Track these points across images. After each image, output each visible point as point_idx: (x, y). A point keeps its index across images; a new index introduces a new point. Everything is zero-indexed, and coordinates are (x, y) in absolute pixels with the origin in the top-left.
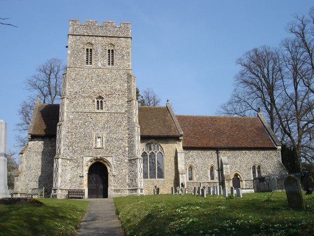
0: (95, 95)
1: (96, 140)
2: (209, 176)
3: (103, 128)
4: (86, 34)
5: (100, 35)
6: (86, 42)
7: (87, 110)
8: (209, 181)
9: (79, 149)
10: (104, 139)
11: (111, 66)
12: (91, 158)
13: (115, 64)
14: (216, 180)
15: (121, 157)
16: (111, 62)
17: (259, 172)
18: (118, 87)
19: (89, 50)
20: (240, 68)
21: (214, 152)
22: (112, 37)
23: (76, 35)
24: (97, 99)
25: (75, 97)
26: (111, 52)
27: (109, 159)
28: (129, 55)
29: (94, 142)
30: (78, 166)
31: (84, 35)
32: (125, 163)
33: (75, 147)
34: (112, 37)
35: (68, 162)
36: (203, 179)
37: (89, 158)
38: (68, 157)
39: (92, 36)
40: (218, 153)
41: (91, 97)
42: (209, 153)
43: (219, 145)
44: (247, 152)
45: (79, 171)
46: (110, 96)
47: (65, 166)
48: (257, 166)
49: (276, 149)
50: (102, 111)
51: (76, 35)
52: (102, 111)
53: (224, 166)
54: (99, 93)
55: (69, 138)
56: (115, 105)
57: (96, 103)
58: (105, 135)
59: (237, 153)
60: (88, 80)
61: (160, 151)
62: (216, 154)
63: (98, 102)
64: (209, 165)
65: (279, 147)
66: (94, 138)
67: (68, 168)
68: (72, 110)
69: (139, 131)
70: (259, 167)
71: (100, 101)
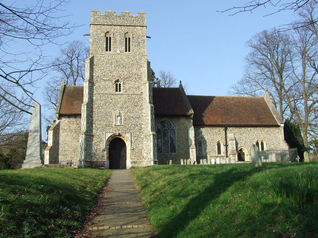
0: (114, 79)
2: (217, 151)
3: (122, 108)
4: (106, 24)
5: (119, 24)
7: (106, 92)
11: (128, 52)
13: (131, 51)
15: (138, 133)
16: (127, 48)
17: (263, 148)
19: (109, 39)
20: (250, 50)
21: (222, 130)
23: (97, 25)
26: (127, 41)
28: (144, 42)
29: (114, 120)
31: (104, 25)
32: (141, 139)
37: (110, 134)
39: (111, 25)
40: (226, 130)
41: (112, 81)
42: (217, 130)
43: (227, 123)
46: (128, 79)
47: (89, 141)
49: (280, 126)
50: (120, 93)
51: (97, 25)
52: (120, 93)
59: (243, 130)
60: (108, 65)
61: (172, 128)
62: (224, 131)
65: (282, 125)
69: (154, 110)
70: (262, 144)
71: (118, 84)
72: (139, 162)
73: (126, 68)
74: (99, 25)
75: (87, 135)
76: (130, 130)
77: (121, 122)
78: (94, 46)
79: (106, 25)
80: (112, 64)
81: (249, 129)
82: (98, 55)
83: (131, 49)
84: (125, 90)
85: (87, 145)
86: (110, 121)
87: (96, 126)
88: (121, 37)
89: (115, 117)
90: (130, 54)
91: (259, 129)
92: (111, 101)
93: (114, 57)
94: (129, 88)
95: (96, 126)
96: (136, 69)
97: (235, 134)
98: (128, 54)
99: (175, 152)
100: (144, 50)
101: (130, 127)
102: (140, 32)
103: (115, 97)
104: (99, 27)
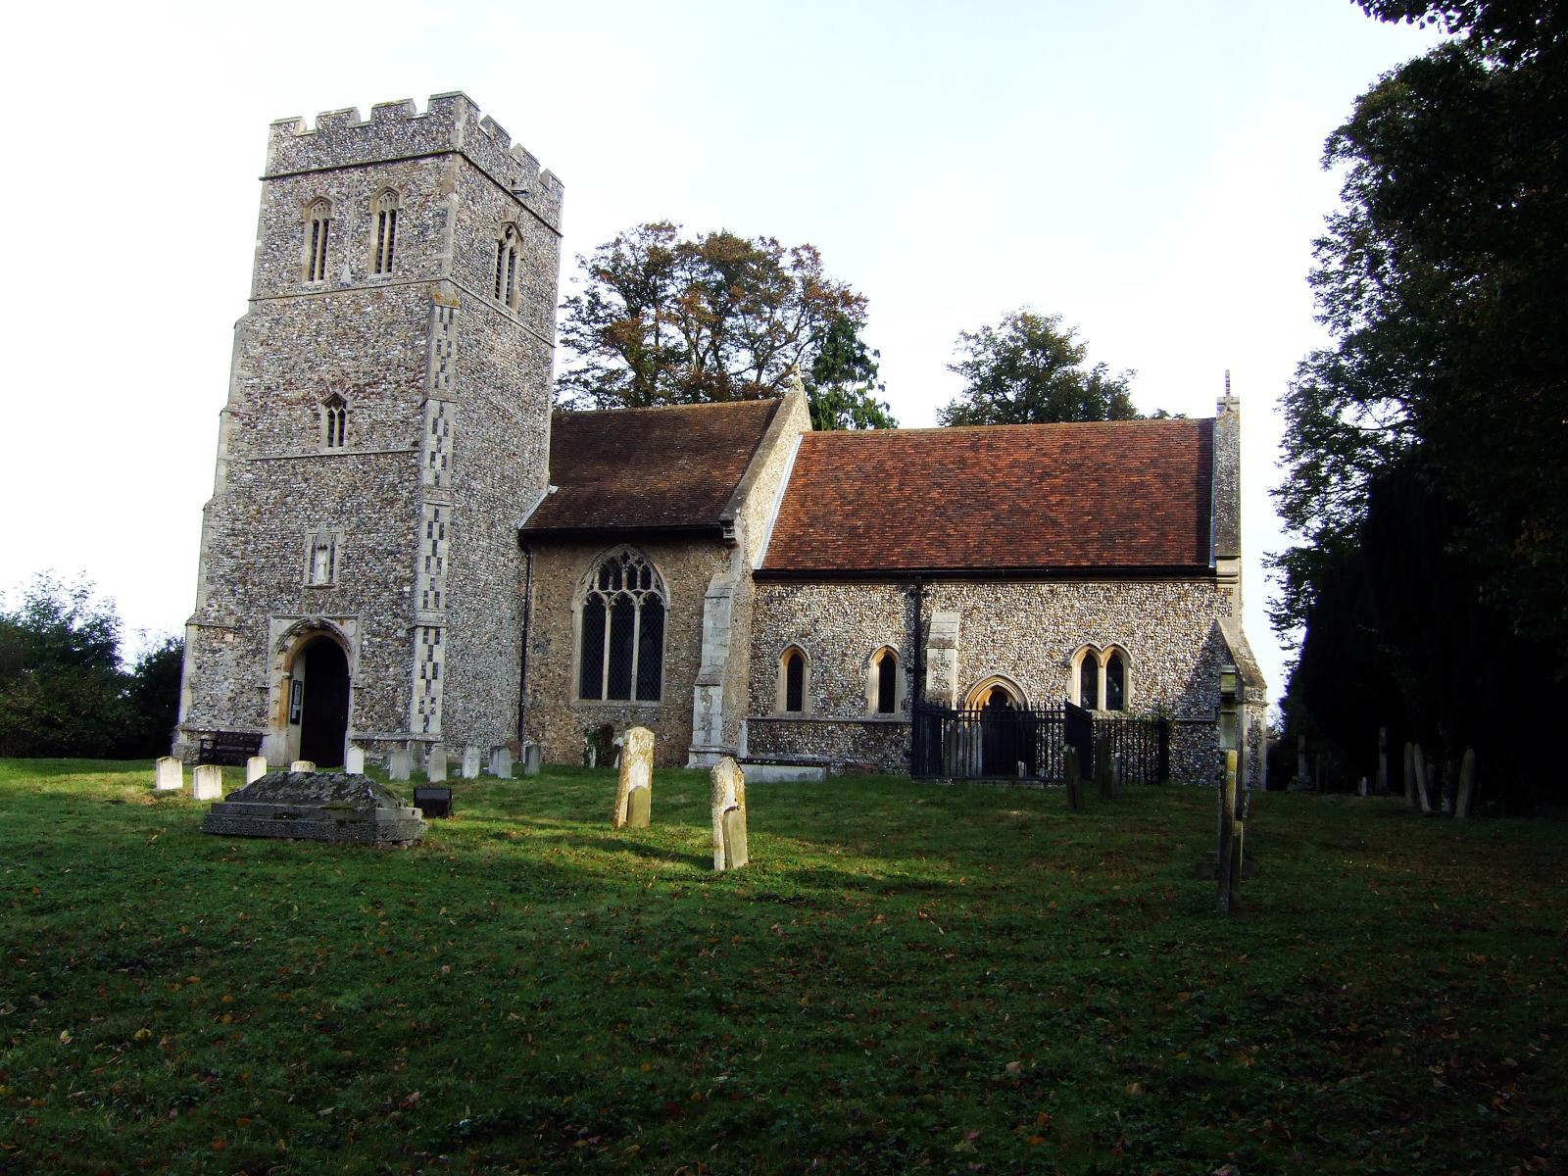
1: (313, 559)
4: (314, 167)
6: (310, 196)
7: (295, 451)
8: (869, 718)
9: (264, 591)
10: (339, 553)
11: (384, 274)
12: (295, 621)
13: (394, 267)
14: (900, 714)
15: (386, 618)
18: (397, 353)
22: (393, 161)
24: (327, 404)
25: (264, 406)
27: (349, 630)
28: (444, 224)
30: (256, 652)
33: (254, 584)
34: (393, 161)
35: (229, 637)
36: (845, 705)
37: (287, 624)
38: (230, 622)
41: (308, 401)
44: (1061, 588)
45: (257, 669)
46: (369, 390)
47: (214, 652)
48: (1104, 659)
52: (337, 450)
53: (932, 653)
54: (333, 384)
55: (237, 553)
56: (382, 422)
57: (324, 421)
58: (341, 540)
59: (1013, 592)
60: (305, 339)
63: (331, 415)
64: (878, 646)
66: (309, 550)
67: (228, 656)
68: (254, 455)
71: (336, 412)
72: (379, 741)
73: (365, 345)
74: (292, 175)
75: (201, 627)
76: (359, 605)
77: (331, 572)
78: (267, 265)
79: (314, 171)
80: (318, 334)
81: (1044, 588)
82: (274, 301)
83: (395, 261)
84: (354, 440)
85: (199, 668)
86: (294, 569)
87: (247, 591)
88: (360, 213)
89: (313, 551)
90: (386, 283)
91: (1098, 590)
92: (304, 485)
93: (328, 300)
94: (373, 428)
95: (247, 591)
96: (404, 345)
97: (967, 615)
98: (379, 284)
99: (609, 698)
100: (440, 256)
101: (362, 591)
102: (432, 180)
103: (318, 468)
104: (288, 184)
